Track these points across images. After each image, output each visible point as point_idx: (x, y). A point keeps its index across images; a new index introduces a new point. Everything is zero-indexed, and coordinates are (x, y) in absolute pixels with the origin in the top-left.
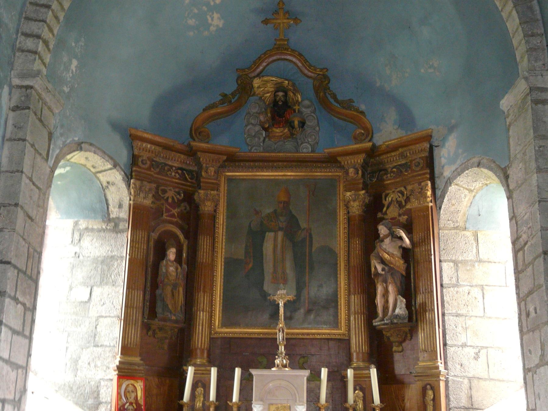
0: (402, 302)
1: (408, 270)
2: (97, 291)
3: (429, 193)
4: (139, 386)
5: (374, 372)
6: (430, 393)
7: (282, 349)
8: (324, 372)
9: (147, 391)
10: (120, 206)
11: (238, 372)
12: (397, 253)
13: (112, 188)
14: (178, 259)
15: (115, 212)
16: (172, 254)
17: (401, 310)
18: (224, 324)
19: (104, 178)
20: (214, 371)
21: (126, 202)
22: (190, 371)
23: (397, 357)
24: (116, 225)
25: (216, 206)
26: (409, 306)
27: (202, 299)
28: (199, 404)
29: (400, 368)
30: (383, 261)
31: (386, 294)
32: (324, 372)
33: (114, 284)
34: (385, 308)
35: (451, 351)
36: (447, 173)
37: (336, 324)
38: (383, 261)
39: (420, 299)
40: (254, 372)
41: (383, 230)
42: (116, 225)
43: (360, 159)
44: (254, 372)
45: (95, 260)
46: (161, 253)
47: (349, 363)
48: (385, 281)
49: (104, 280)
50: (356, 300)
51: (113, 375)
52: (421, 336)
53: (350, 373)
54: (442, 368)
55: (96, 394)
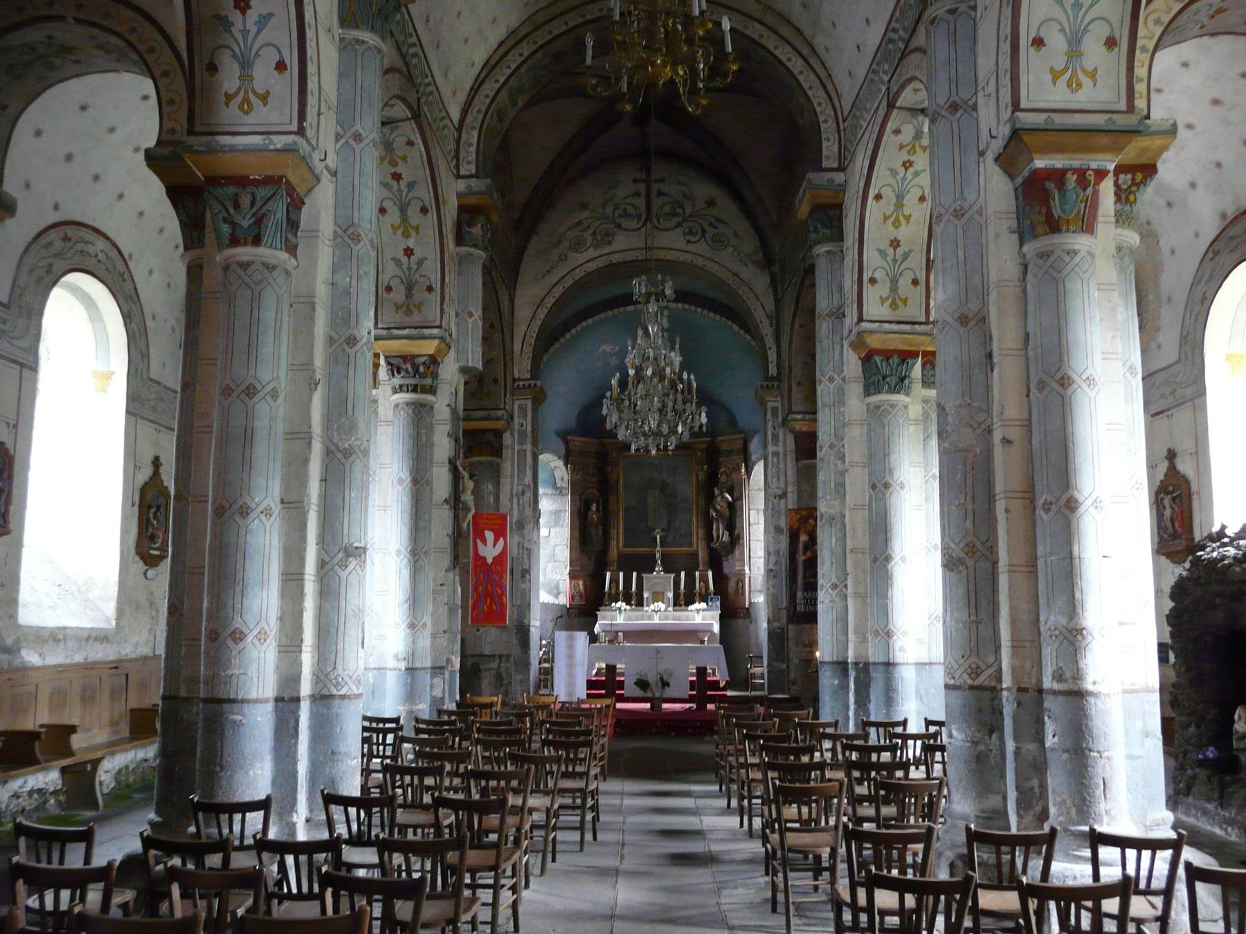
0: (727, 533)
1: (731, 515)
2: (553, 530)
3: (743, 470)
4: (581, 583)
5: (710, 573)
6: (740, 584)
7: (659, 562)
8: (683, 574)
9: (585, 585)
10: (562, 480)
11: (635, 574)
12: (725, 505)
13: (558, 470)
14: (598, 509)
15: (559, 484)
16: (594, 507)
17: (726, 538)
18: (625, 546)
19: (553, 465)
20: (621, 574)
21: (566, 477)
22: (608, 574)
23: (725, 563)
24: (561, 491)
25: (618, 475)
26: (731, 535)
27: (613, 532)
28: (613, 592)
29: (726, 570)
30: (716, 510)
31: (718, 529)
32: (683, 574)
33: (562, 526)
34: (718, 537)
35: (752, 560)
36: (754, 458)
37: (691, 545)
38: (716, 510)
39: (737, 531)
40: (644, 575)
41: (716, 492)
42: (561, 491)
43: (704, 446)
44: (644, 575)
45: (550, 512)
46: (588, 507)
47: (697, 569)
48: (718, 521)
49: (556, 524)
50: (701, 532)
51: (567, 577)
52: (737, 553)
53: (697, 574)
54: (747, 571)
55: (557, 587)
